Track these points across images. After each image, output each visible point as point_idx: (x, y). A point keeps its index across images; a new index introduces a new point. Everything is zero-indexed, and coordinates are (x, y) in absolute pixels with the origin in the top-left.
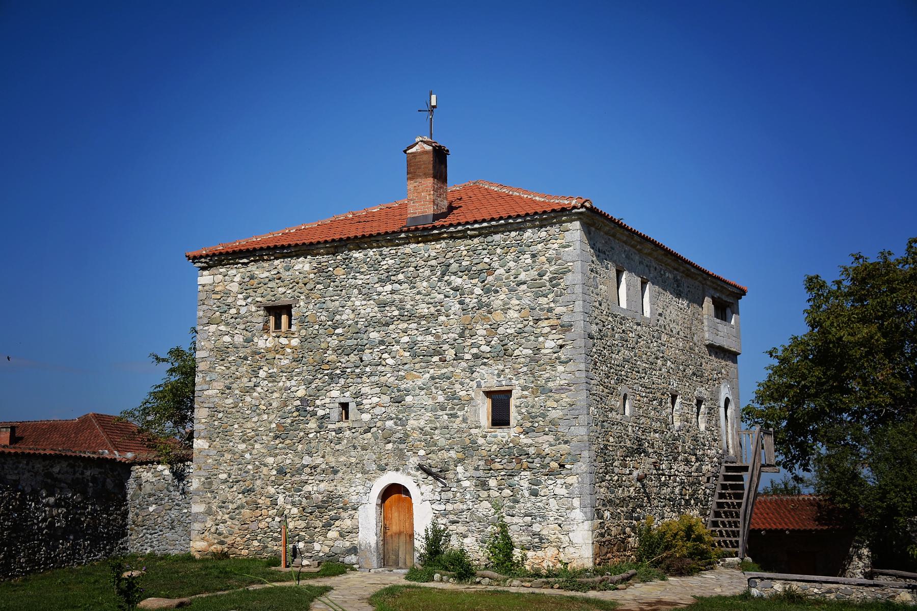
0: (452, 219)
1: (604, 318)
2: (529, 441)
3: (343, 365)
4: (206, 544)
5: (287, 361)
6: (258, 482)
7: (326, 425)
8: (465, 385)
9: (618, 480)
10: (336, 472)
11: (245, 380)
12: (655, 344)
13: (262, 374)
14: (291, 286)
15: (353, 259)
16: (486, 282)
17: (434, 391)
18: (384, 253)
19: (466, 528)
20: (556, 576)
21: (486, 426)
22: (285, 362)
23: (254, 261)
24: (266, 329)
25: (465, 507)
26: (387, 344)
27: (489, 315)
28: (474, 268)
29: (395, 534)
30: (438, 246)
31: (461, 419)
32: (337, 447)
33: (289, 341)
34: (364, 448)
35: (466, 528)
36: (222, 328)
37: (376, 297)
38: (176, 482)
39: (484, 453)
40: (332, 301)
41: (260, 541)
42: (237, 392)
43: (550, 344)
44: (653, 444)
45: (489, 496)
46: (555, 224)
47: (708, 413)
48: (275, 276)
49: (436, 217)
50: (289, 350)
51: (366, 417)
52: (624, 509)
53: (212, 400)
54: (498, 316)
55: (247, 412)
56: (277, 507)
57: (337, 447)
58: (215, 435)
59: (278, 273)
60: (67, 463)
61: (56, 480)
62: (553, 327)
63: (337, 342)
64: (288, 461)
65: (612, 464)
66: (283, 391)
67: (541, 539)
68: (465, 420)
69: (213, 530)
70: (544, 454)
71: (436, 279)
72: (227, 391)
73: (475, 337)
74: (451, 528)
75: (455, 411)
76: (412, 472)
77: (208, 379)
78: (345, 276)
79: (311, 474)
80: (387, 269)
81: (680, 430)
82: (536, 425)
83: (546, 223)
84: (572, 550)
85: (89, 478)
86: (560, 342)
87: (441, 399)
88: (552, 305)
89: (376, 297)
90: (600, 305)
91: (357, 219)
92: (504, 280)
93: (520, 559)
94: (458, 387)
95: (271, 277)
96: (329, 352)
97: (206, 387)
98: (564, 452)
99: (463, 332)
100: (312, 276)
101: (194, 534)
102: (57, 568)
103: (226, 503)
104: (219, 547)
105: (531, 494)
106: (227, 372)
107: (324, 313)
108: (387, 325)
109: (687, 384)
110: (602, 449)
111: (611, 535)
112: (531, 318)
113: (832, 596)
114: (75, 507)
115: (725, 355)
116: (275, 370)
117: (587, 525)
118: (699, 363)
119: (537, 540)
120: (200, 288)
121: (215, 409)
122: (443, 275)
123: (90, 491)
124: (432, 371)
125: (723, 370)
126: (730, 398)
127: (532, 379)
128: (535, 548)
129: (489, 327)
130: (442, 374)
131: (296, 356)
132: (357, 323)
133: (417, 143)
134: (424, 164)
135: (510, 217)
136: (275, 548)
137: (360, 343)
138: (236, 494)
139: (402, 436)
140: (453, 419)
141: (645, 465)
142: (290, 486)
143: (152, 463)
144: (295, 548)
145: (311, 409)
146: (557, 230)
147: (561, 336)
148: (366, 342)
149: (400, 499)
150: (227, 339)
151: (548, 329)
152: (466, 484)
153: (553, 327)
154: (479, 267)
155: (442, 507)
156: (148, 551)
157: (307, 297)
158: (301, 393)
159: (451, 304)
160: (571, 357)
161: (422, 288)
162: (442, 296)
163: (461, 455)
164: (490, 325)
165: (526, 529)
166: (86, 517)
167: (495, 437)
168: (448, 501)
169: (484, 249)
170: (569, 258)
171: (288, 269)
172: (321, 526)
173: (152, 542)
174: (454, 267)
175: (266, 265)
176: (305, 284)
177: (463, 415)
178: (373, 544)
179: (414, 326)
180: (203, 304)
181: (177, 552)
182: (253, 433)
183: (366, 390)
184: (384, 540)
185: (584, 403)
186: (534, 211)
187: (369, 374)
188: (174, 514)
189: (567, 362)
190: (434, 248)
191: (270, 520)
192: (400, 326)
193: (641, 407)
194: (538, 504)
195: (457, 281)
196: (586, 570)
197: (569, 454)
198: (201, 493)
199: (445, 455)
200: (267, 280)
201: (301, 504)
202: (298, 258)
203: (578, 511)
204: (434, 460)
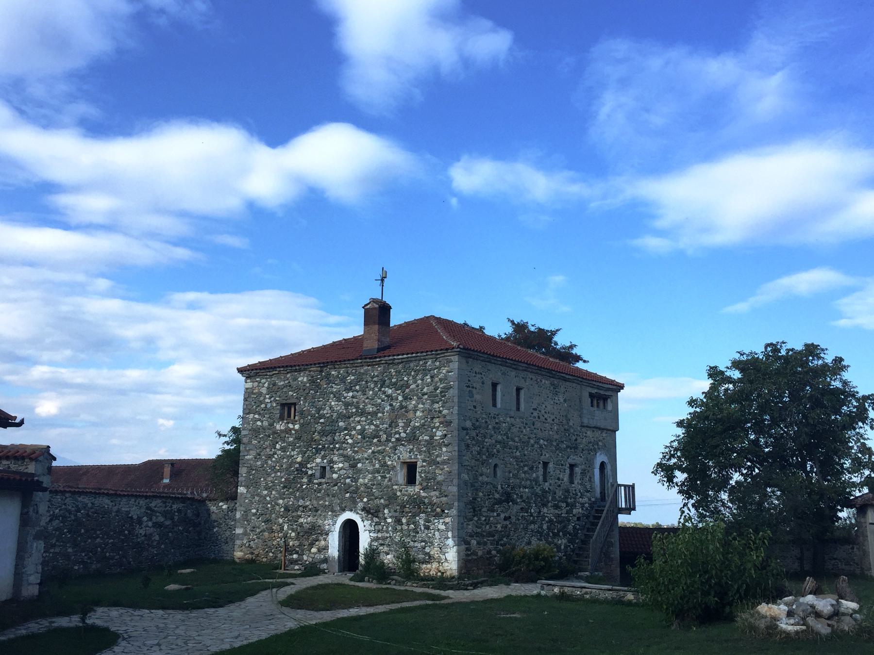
3: (324, 443)
4: (243, 553)
10: (317, 511)
13: (278, 446)
16: (405, 392)
19: (388, 549)
22: (291, 439)
25: (388, 535)
26: (349, 430)
31: (388, 479)
33: (294, 426)
34: (333, 496)
35: (388, 549)
36: (257, 416)
37: (344, 400)
39: (400, 501)
41: (273, 553)
43: (439, 433)
48: (287, 384)
50: (293, 432)
51: (335, 476)
53: (249, 462)
56: (284, 532)
58: (251, 485)
59: (289, 382)
60: (161, 501)
62: (441, 423)
64: (291, 503)
66: (289, 458)
68: (390, 480)
69: (247, 545)
72: (258, 457)
73: (398, 427)
78: (326, 386)
79: (303, 511)
84: (446, 564)
85: (176, 510)
87: (377, 466)
88: (441, 409)
89: (344, 400)
97: (246, 453)
99: (391, 424)
100: (308, 385)
104: (250, 556)
105: (425, 528)
108: (349, 418)
116: (285, 444)
119: (427, 557)
122: (382, 387)
123: (176, 518)
127: (428, 455)
128: (429, 562)
138: (261, 523)
142: (291, 518)
147: (445, 429)
148: (336, 428)
150: (259, 423)
152: (389, 520)
154: (402, 383)
155: (375, 535)
157: (305, 398)
158: (299, 459)
163: (387, 502)
165: (422, 550)
167: (407, 491)
168: (379, 531)
174: (387, 382)
176: (304, 390)
177: (390, 476)
182: (272, 484)
183: (335, 459)
185: (456, 472)
189: (448, 446)
192: (356, 419)
194: (429, 535)
195: (390, 391)
196: (454, 577)
197: (447, 503)
199: (377, 501)
201: (297, 530)
203: (450, 540)
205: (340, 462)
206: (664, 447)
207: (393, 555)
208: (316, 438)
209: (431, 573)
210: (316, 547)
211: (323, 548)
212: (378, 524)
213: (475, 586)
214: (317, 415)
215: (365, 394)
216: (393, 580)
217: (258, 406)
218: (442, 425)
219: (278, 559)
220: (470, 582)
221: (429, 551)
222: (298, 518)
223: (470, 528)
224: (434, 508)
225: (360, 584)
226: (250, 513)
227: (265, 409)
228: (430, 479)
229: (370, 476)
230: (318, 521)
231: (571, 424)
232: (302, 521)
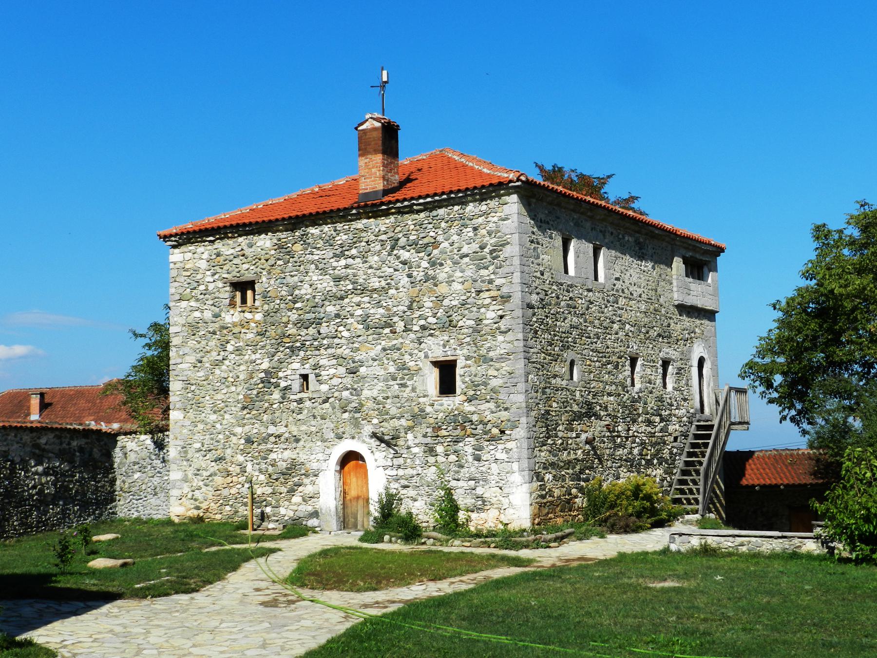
0: (399, 195)
2: (472, 409)
3: (303, 338)
6: (229, 452)
7: (288, 396)
8: (414, 355)
10: (297, 441)
11: (214, 354)
13: (230, 348)
14: (254, 262)
15: (310, 235)
17: (386, 362)
18: (338, 229)
19: (416, 492)
20: (494, 536)
22: (250, 336)
24: (232, 304)
25: (415, 472)
27: (435, 288)
28: (420, 242)
30: (387, 221)
31: (410, 388)
32: (299, 417)
33: (254, 316)
34: (323, 418)
35: (416, 492)
37: (331, 272)
39: (432, 421)
40: (292, 276)
42: (207, 365)
43: (491, 315)
45: (436, 462)
46: (494, 197)
48: (239, 253)
49: (386, 192)
50: (253, 325)
51: (324, 388)
53: (185, 373)
54: (443, 289)
55: (217, 384)
56: (246, 474)
57: (299, 417)
58: (189, 407)
59: (242, 250)
61: (44, 450)
64: (255, 431)
66: (249, 364)
67: (484, 501)
68: (414, 390)
69: (190, 496)
70: (486, 420)
72: (199, 365)
75: (405, 381)
76: (366, 440)
77: (181, 353)
78: (302, 252)
79: (275, 443)
80: (341, 244)
83: (485, 196)
85: (76, 448)
86: (500, 313)
87: (392, 369)
88: (492, 277)
89: (331, 272)
92: (448, 254)
93: (464, 520)
94: (407, 358)
95: (235, 254)
97: (179, 361)
99: (411, 305)
101: (172, 500)
102: (48, 530)
103: (201, 471)
107: (285, 288)
112: (473, 290)
113: (744, 549)
114: (63, 475)
116: (241, 344)
117: (526, 488)
119: (480, 503)
121: (188, 382)
122: (393, 248)
123: (77, 459)
124: (383, 343)
127: (475, 349)
128: (480, 510)
129: (435, 299)
130: (393, 346)
131: (260, 330)
132: (314, 297)
133: (367, 120)
134: (374, 140)
137: (318, 316)
142: (257, 454)
144: (263, 513)
146: (497, 203)
147: (501, 307)
148: (323, 315)
150: (197, 314)
151: (488, 301)
152: (415, 450)
153: (494, 298)
154: (426, 241)
155: (394, 472)
157: (269, 273)
158: (265, 365)
160: (510, 327)
161: (373, 263)
162: (392, 270)
163: (410, 423)
164: (436, 297)
166: (75, 484)
168: (399, 467)
170: (507, 231)
171: (250, 246)
172: (286, 491)
173: (138, 507)
174: (403, 241)
175: (230, 242)
176: (267, 260)
178: (333, 509)
179: (367, 299)
180: (175, 281)
182: (223, 404)
184: (344, 504)
185: (522, 372)
186: (474, 185)
187: (326, 346)
188: (156, 480)
189: (506, 332)
190: (384, 223)
194: (481, 468)
195: (405, 255)
196: (524, 530)
197: (509, 420)
198: (178, 462)
199: (395, 423)
200: (232, 257)
203: (517, 474)
204: (387, 428)
205: (330, 367)
206: (759, 338)
207: (424, 502)
208: (289, 332)
209: (486, 525)
211: (310, 495)
213: (560, 540)
214: (290, 298)
215: (366, 262)
218: (494, 302)
219: (240, 514)
222: (269, 452)
223: (544, 455)
224: (488, 428)
225: (380, 546)
228: (478, 385)
229: (381, 384)
231: (662, 300)
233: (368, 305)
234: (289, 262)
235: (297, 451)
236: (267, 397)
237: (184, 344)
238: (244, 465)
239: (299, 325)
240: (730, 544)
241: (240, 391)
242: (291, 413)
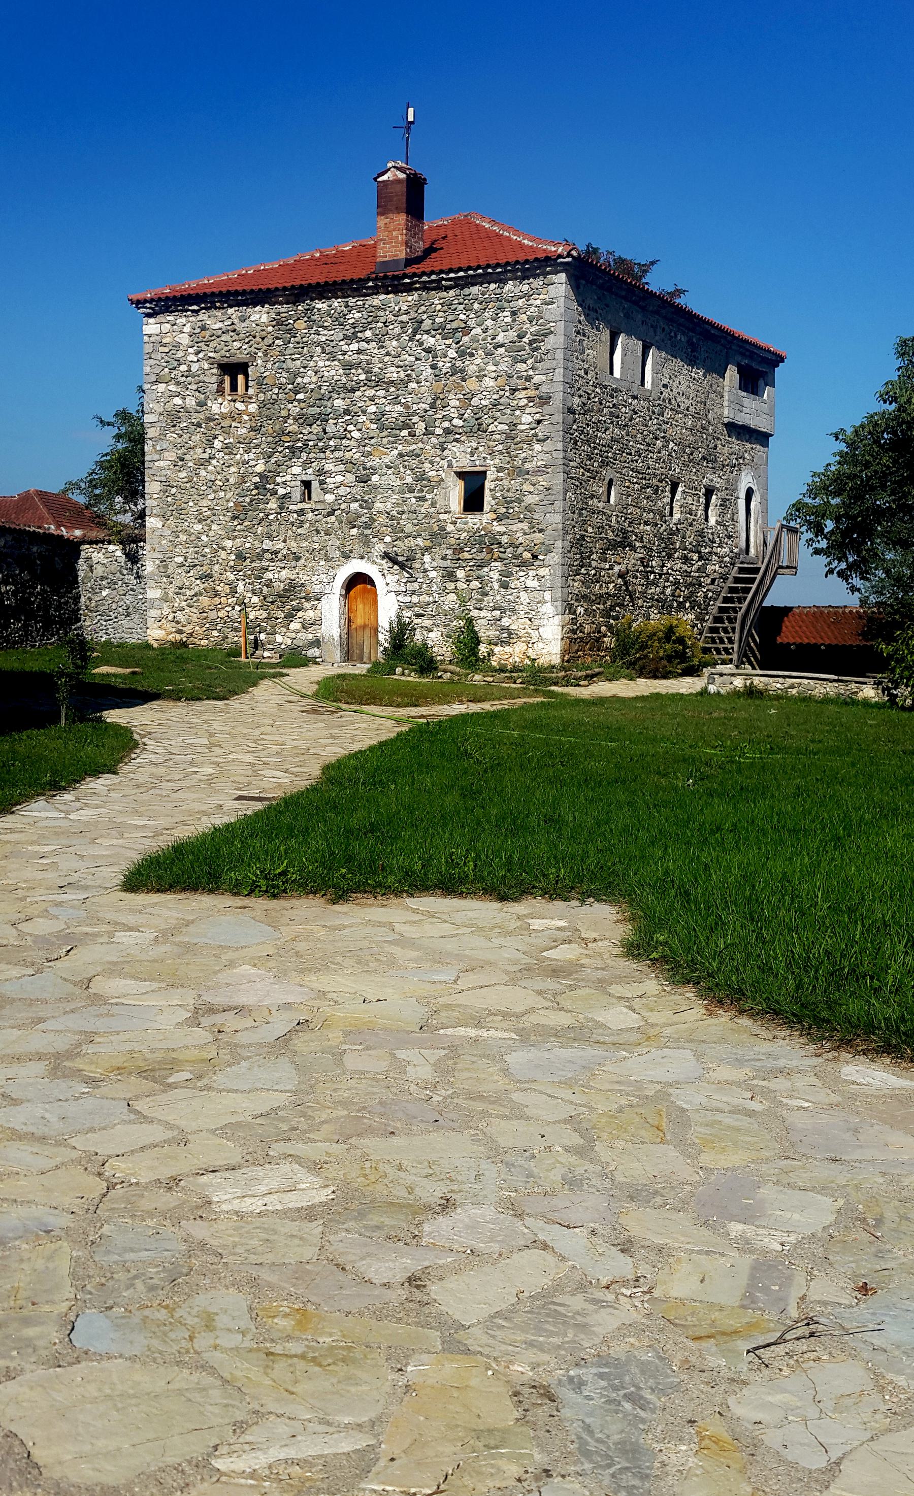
0: (425, 266)
1: (589, 389)
2: (503, 529)
3: (305, 438)
4: (163, 632)
5: (244, 431)
6: (217, 567)
9: (595, 575)
10: (298, 559)
12: (655, 421)
13: (217, 444)
14: (247, 340)
15: (315, 310)
17: (402, 470)
18: (350, 304)
21: (457, 511)
23: (206, 308)
24: (220, 391)
25: (431, 599)
27: (463, 383)
28: (448, 326)
29: (360, 627)
30: (410, 298)
31: (430, 502)
33: (247, 406)
34: (327, 533)
37: (341, 357)
38: (129, 565)
39: (453, 541)
43: (527, 419)
44: (642, 537)
45: (456, 588)
46: (539, 275)
47: (721, 505)
48: (229, 328)
49: (409, 262)
50: (246, 418)
52: (601, 607)
53: (164, 472)
54: (472, 385)
55: (202, 488)
56: (237, 595)
58: (169, 513)
59: (233, 324)
63: (298, 409)
64: (248, 545)
65: (589, 557)
67: (510, 634)
68: (433, 505)
69: (170, 618)
70: (517, 543)
71: (407, 338)
72: (180, 463)
73: (447, 409)
74: (416, 621)
78: (306, 331)
79: (272, 560)
80: (353, 324)
81: (680, 522)
82: (511, 511)
83: (528, 274)
84: (541, 645)
86: (538, 417)
87: (409, 479)
88: (531, 372)
89: (341, 357)
90: (586, 373)
91: (324, 260)
92: (481, 342)
93: (486, 654)
96: (290, 421)
97: (157, 457)
98: (538, 542)
99: (435, 402)
100: (270, 329)
101: (150, 622)
102: (10, 648)
104: (178, 637)
105: (501, 587)
106: (179, 440)
107: (284, 374)
108: (353, 391)
109: (694, 470)
110: (578, 539)
111: (584, 633)
112: (507, 388)
114: (23, 584)
115: (750, 437)
116: (231, 440)
117: (558, 619)
118: (712, 446)
120: (146, 338)
122: (415, 333)
124: (400, 447)
125: (746, 455)
126: (755, 488)
127: (508, 459)
128: (503, 643)
131: (254, 425)
132: (320, 387)
133: (389, 170)
134: (397, 195)
135: (488, 266)
136: (236, 639)
139: (367, 520)
140: (420, 503)
141: (631, 560)
142: (249, 572)
143: (103, 542)
144: (256, 640)
145: (271, 486)
146: (541, 283)
147: (539, 410)
148: (330, 410)
149: (365, 591)
150: (178, 401)
151: (526, 401)
152: (432, 574)
154: (455, 325)
155: (408, 599)
156: (103, 639)
157: (266, 355)
158: (260, 468)
159: (422, 368)
161: (391, 348)
162: (412, 359)
163: (428, 543)
164: (464, 395)
166: (36, 598)
168: (413, 592)
169: (460, 304)
173: (107, 629)
174: (427, 324)
175: (218, 313)
176: (263, 339)
178: (337, 638)
179: (382, 393)
180: (150, 358)
181: (133, 641)
182: (209, 512)
183: (329, 467)
184: (348, 633)
185: (560, 488)
186: (515, 259)
188: (129, 599)
189: (544, 441)
190: (406, 300)
191: (230, 608)
192: (367, 393)
193: (630, 495)
195: (430, 341)
196: (553, 667)
197: (543, 544)
200: (220, 332)
202: (255, 307)
203: (549, 604)
204: (401, 547)
208: (289, 429)
209: (510, 660)
210: (300, 620)
212: (412, 579)
213: (591, 678)
214: (290, 386)
216: (445, 671)
217: (175, 369)
218: (531, 404)
220: (583, 673)
221: (507, 624)
226: (173, 563)
227: (188, 374)
230: (301, 576)
232: (271, 576)
233: (384, 400)
234: (289, 342)
235: (297, 571)
236: (261, 506)
237: (162, 437)
238: (235, 584)
239: (301, 421)
240: (779, 686)
241: (230, 498)
242: (290, 526)
